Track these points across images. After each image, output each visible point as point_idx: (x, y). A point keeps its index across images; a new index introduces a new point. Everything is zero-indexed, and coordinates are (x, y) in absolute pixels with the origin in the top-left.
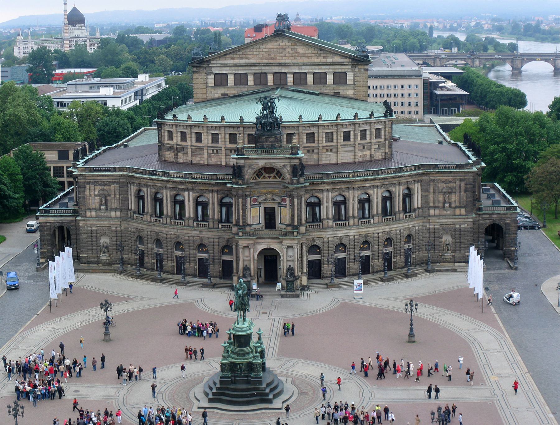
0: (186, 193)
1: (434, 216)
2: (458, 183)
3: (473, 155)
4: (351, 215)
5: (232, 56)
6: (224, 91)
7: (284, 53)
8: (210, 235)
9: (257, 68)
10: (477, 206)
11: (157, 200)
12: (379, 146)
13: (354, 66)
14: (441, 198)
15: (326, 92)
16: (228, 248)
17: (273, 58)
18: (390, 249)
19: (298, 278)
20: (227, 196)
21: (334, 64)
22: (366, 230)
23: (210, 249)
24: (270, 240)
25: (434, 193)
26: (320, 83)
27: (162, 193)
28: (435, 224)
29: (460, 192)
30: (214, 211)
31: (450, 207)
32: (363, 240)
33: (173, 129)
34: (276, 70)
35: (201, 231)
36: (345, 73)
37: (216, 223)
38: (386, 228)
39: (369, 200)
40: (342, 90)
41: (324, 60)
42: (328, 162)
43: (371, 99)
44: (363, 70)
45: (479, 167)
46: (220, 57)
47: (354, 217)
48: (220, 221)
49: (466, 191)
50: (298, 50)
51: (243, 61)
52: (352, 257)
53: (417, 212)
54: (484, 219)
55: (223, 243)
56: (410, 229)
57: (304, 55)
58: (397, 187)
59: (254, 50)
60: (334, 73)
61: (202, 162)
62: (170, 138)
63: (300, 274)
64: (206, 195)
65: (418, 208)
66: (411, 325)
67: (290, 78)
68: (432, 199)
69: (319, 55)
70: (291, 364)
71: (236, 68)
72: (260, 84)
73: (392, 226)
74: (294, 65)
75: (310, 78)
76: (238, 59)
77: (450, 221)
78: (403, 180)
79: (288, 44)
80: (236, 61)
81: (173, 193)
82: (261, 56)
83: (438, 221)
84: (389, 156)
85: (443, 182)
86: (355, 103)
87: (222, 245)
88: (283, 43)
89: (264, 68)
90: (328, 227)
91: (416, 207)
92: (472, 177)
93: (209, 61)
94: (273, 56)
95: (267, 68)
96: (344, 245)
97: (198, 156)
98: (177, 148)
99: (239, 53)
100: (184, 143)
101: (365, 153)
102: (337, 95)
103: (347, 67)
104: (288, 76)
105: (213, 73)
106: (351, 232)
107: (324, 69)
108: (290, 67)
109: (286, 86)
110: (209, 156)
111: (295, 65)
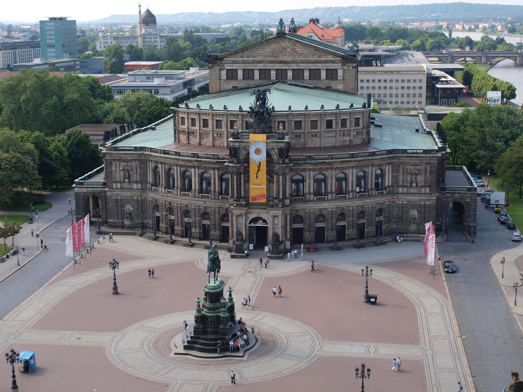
0: (193, 170)
1: (403, 193)
2: (424, 166)
3: (440, 142)
4: (329, 191)
5: (241, 54)
6: (233, 83)
7: (285, 52)
8: (211, 203)
9: (262, 65)
10: (441, 186)
11: (168, 174)
12: (357, 132)
13: (343, 64)
14: (409, 179)
15: (320, 86)
16: (225, 217)
17: (276, 57)
18: (362, 221)
19: (283, 242)
20: (226, 173)
21: (326, 62)
22: (343, 203)
23: (212, 216)
24: (259, 211)
25: (403, 173)
26: (315, 79)
27: (174, 170)
28: (403, 200)
29: (426, 173)
30: (215, 185)
31: (417, 186)
32: (339, 212)
33: (185, 116)
34: (279, 66)
35: (205, 202)
36: (336, 70)
37: (217, 194)
38: (359, 203)
39: (346, 179)
40: (333, 84)
41: (318, 59)
42: (313, 146)
43: (360, 92)
44: (351, 68)
45: (444, 152)
46: (231, 55)
47: (331, 192)
48: (221, 193)
49: (430, 173)
50: (297, 50)
51: (251, 59)
52: (330, 226)
53: (388, 189)
54: (446, 198)
55: (223, 212)
56: (381, 203)
57: (301, 54)
58: (370, 168)
59: (260, 50)
60: (327, 70)
61: (208, 144)
62: (183, 123)
63: (284, 239)
64: (209, 171)
65: (389, 186)
66: (367, 287)
67: (290, 74)
68: (401, 179)
69: (315, 54)
70: (262, 317)
71: (245, 65)
72: (265, 79)
73: (365, 201)
74: (293, 63)
75: (307, 74)
76: (246, 57)
77: (416, 198)
78: (376, 162)
79: (289, 45)
80: (245, 59)
81: (183, 169)
82: (266, 54)
83: (406, 198)
84: (366, 141)
85: (411, 165)
86: (342, 96)
87: (221, 214)
88: (285, 44)
89: (268, 65)
90: (310, 201)
91: (387, 185)
92: (436, 161)
93: (222, 59)
94: (275, 55)
95: (271, 65)
96: (323, 216)
97: (205, 139)
98: (188, 132)
99: (247, 52)
100: (193, 128)
101: (345, 138)
102: (328, 89)
103: (338, 65)
104: (288, 72)
105: (225, 69)
106: (329, 206)
107: (318, 66)
108: (290, 65)
109: (286, 81)
110: (214, 139)
111: (293, 62)
